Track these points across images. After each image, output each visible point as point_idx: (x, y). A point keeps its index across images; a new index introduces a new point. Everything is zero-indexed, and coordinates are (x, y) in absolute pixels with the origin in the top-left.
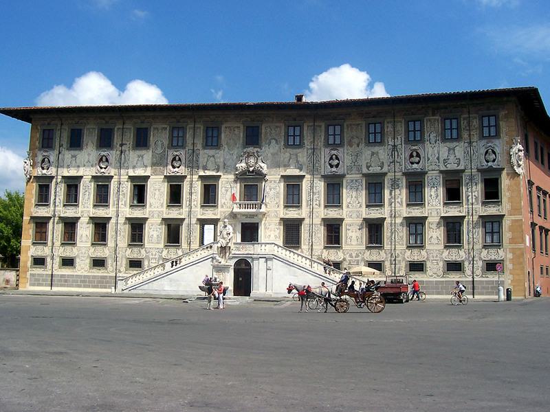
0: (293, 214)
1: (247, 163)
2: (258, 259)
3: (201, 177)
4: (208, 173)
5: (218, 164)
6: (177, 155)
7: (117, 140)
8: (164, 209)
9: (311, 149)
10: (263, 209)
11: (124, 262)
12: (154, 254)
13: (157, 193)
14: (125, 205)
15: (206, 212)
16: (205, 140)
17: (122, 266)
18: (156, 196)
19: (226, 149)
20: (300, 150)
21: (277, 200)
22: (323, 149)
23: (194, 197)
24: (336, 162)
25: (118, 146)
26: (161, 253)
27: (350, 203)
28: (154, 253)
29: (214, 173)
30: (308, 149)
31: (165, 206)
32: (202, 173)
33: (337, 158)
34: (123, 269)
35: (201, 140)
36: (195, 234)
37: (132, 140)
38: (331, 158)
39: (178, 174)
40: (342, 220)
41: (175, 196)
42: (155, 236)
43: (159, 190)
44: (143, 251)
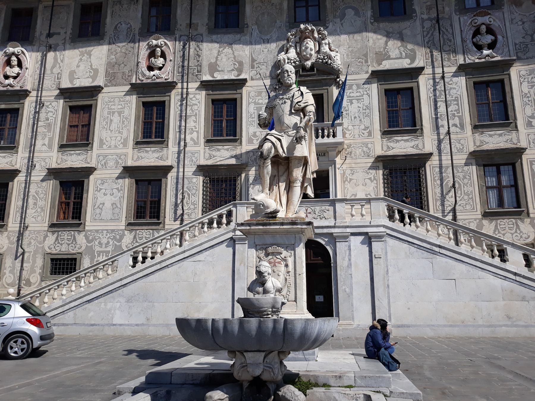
0: (403, 146)
1: (297, 54)
2: (345, 238)
3: (205, 85)
4: (218, 76)
5: (240, 59)
6: (157, 46)
7: (41, 26)
8: (130, 149)
9: (430, 19)
10: (339, 138)
11: (39, 262)
12: (103, 247)
13: (116, 118)
14: (50, 146)
15: (218, 153)
16: (213, 19)
17: (33, 271)
18: (114, 126)
19: (256, 33)
20: (407, 24)
21: (366, 122)
22: (456, 18)
23: (191, 123)
24: (489, 39)
25: (43, 38)
26: (120, 241)
27: (532, 117)
28: (104, 241)
29: (232, 76)
30: (423, 20)
31: (131, 143)
32: (207, 77)
33: (490, 31)
34: (35, 278)
35: (206, 20)
36: (193, 199)
37: (70, 26)
38: (477, 32)
39: (158, 81)
40: (519, 152)
41: (153, 126)
42: (108, 205)
43: (120, 113)
44: (81, 238)
